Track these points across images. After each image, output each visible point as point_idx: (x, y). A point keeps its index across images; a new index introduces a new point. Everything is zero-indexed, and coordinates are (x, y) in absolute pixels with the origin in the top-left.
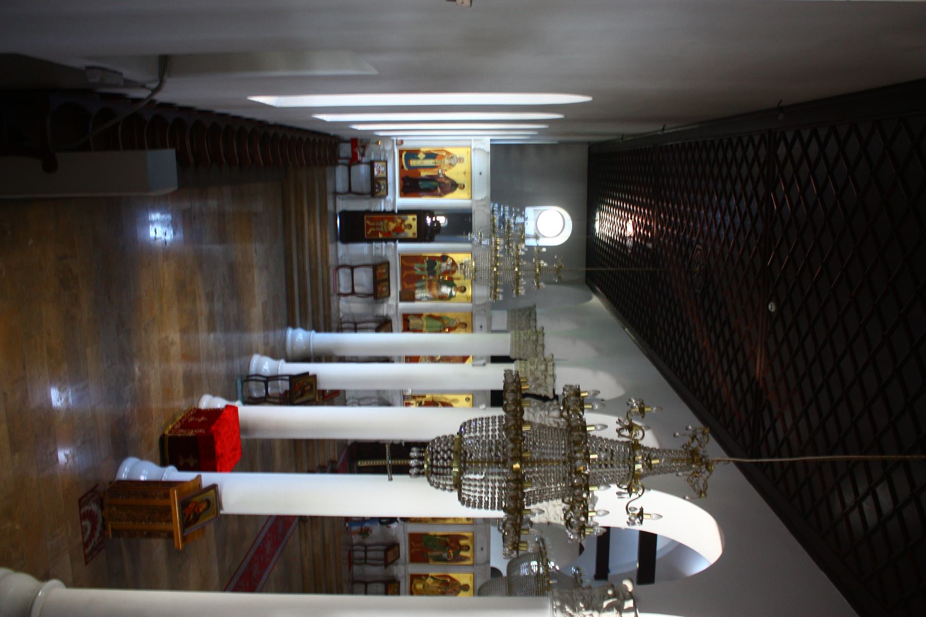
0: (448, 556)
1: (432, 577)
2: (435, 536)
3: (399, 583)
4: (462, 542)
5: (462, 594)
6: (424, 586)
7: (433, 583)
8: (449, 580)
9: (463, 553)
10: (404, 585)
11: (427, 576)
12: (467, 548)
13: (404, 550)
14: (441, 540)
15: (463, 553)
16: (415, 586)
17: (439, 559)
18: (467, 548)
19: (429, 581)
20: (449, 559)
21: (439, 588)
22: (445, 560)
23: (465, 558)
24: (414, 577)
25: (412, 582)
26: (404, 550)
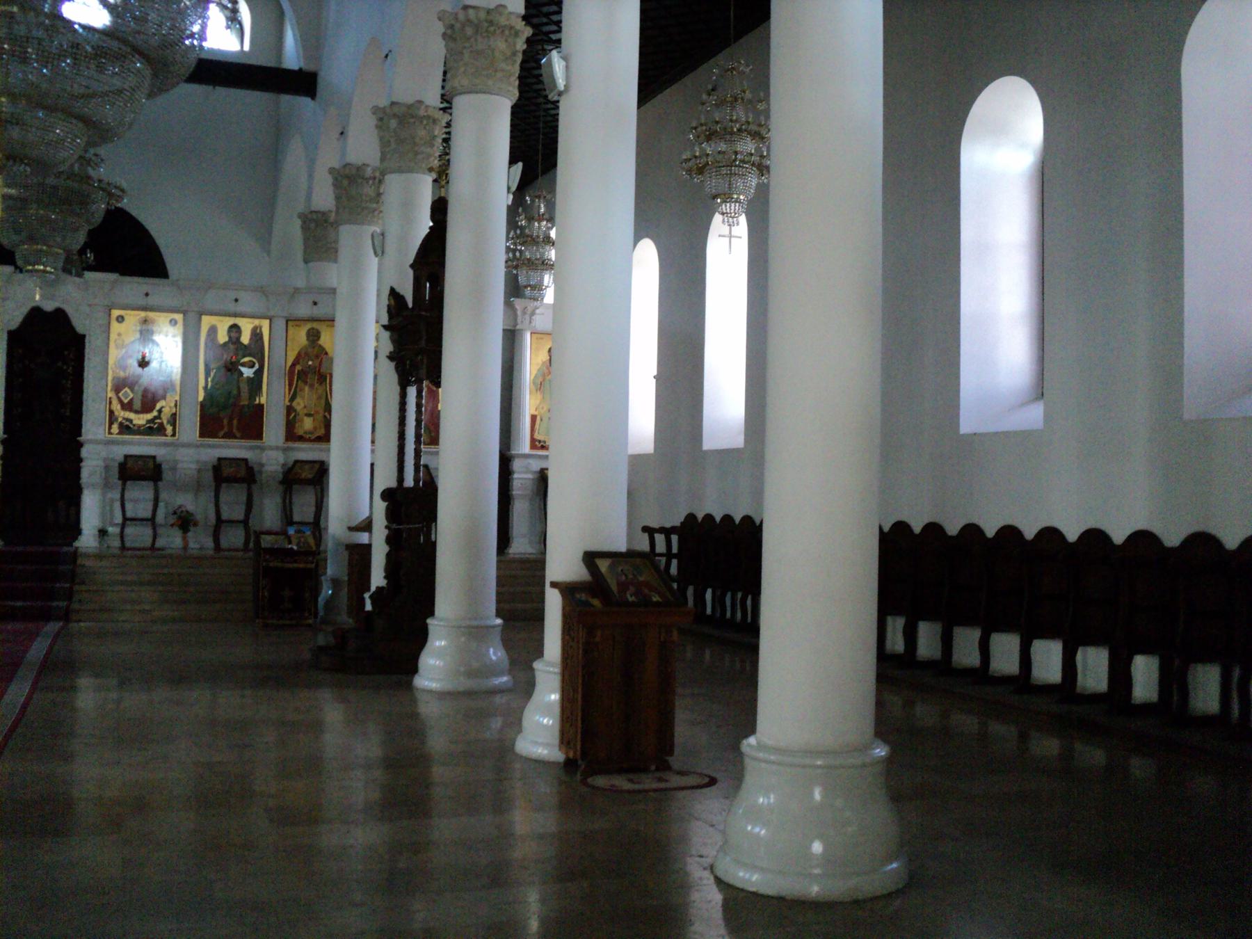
0: (252, 366)
1: (292, 399)
2: (205, 388)
3: (296, 462)
4: (222, 337)
5: (324, 340)
6: (308, 415)
7: (303, 398)
8: (298, 368)
9: (245, 339)
10: (306, 452)
11: (290, 409)
12: (234, 330)
13: (234, 449)
14: (215, 376)
15: (245, 339)
16: (306, 433)
17: (255, 384)
18: (235, 328)
19: (299, 404)
20: (257, 366)
21: (312, 386)
22: (259, 373)
23: (257, 335)
24: (292, 434)
25: (301, 439)
26: (234, 449)
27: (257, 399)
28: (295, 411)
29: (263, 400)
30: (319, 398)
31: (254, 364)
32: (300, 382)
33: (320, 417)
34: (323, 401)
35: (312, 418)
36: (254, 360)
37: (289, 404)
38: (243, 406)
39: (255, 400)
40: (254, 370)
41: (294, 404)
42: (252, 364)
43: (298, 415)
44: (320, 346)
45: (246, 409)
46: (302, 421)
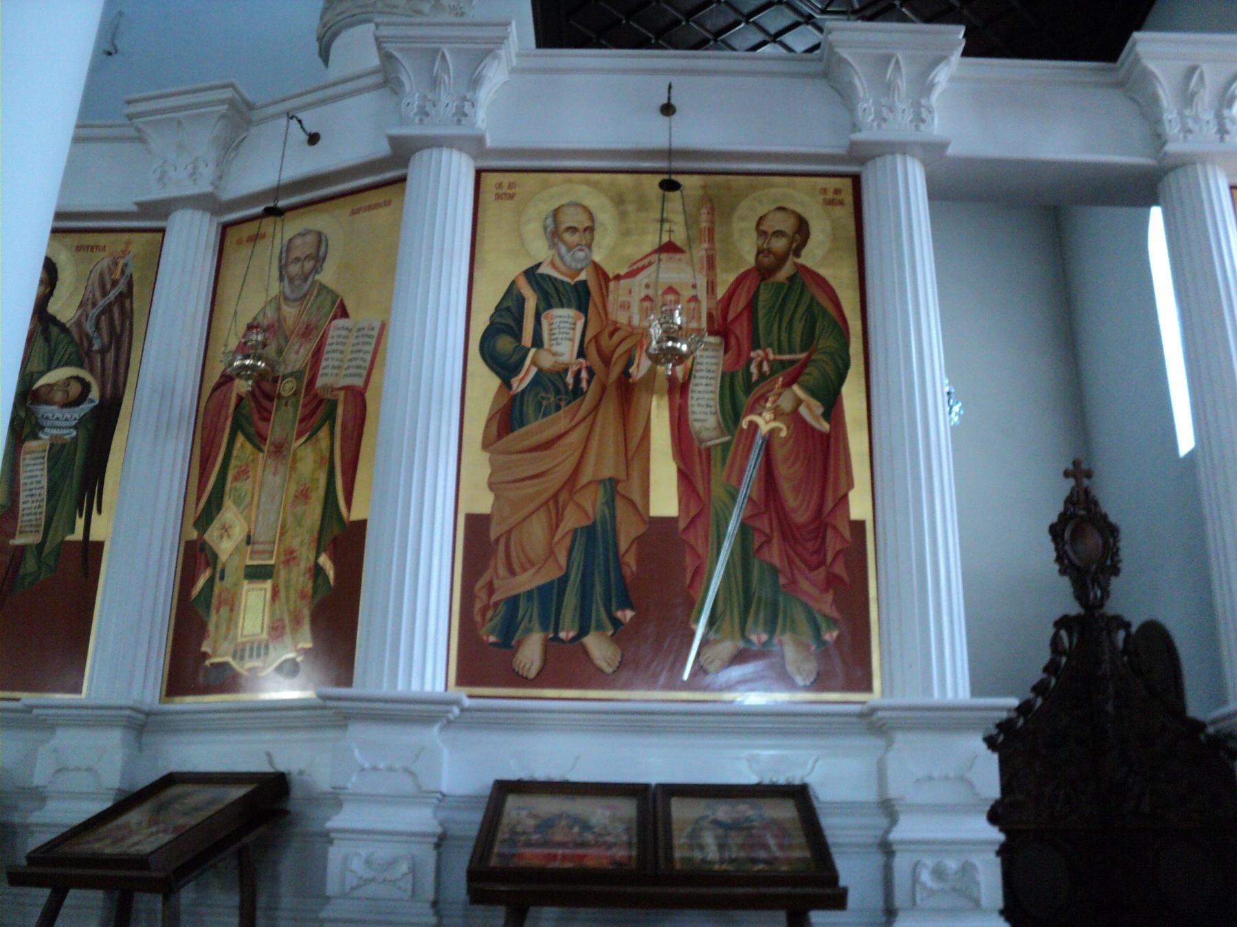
6: (256, 574)
20: (95, 394)
27: (80, 523)
28: (212, 559)
29: (100, 528)
30: (304, 495)
31: (86, 387)
32: (240, 439)
33: (299, 577)
34: (314, 511)
35: (268, 585)
36: (88, 377)
37: (194, 535)
38: (22, 549)
39: (72, 530)
40: (86, 407)
41: (211, 536)
42: (75, 389)
43: (222, 578)
44: (322, 287)
45: (30, 564)
46: (232, 604)
